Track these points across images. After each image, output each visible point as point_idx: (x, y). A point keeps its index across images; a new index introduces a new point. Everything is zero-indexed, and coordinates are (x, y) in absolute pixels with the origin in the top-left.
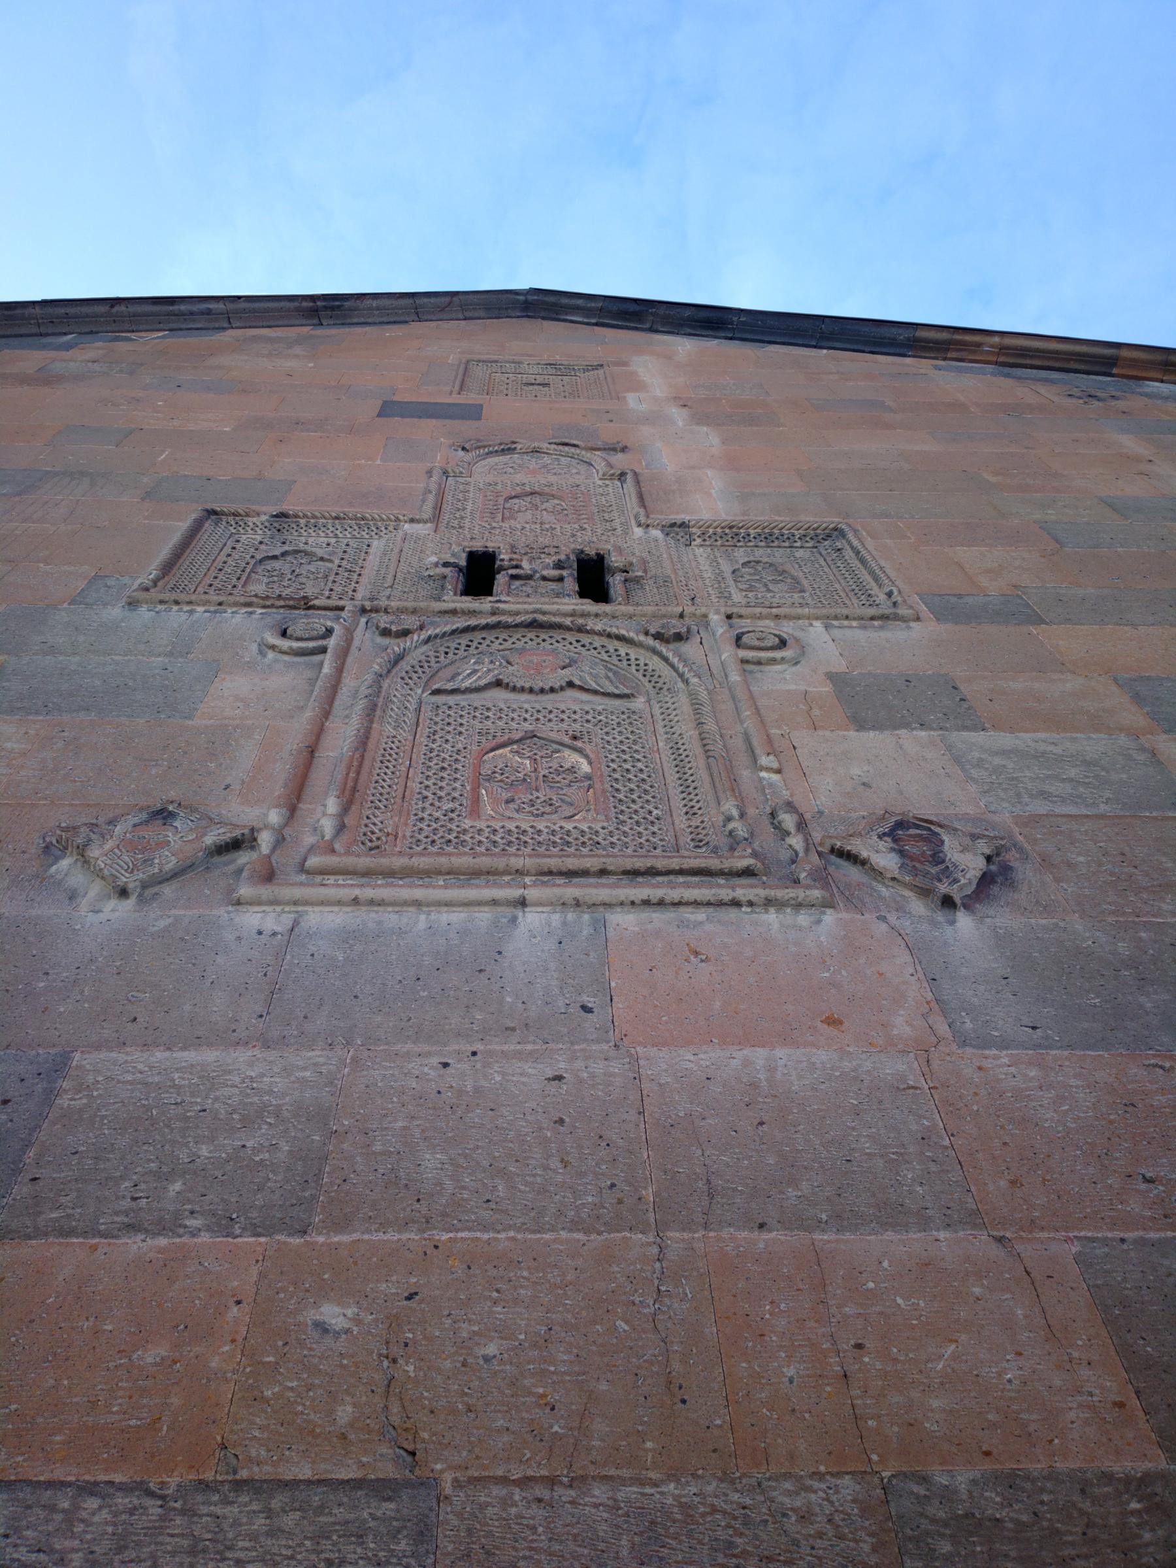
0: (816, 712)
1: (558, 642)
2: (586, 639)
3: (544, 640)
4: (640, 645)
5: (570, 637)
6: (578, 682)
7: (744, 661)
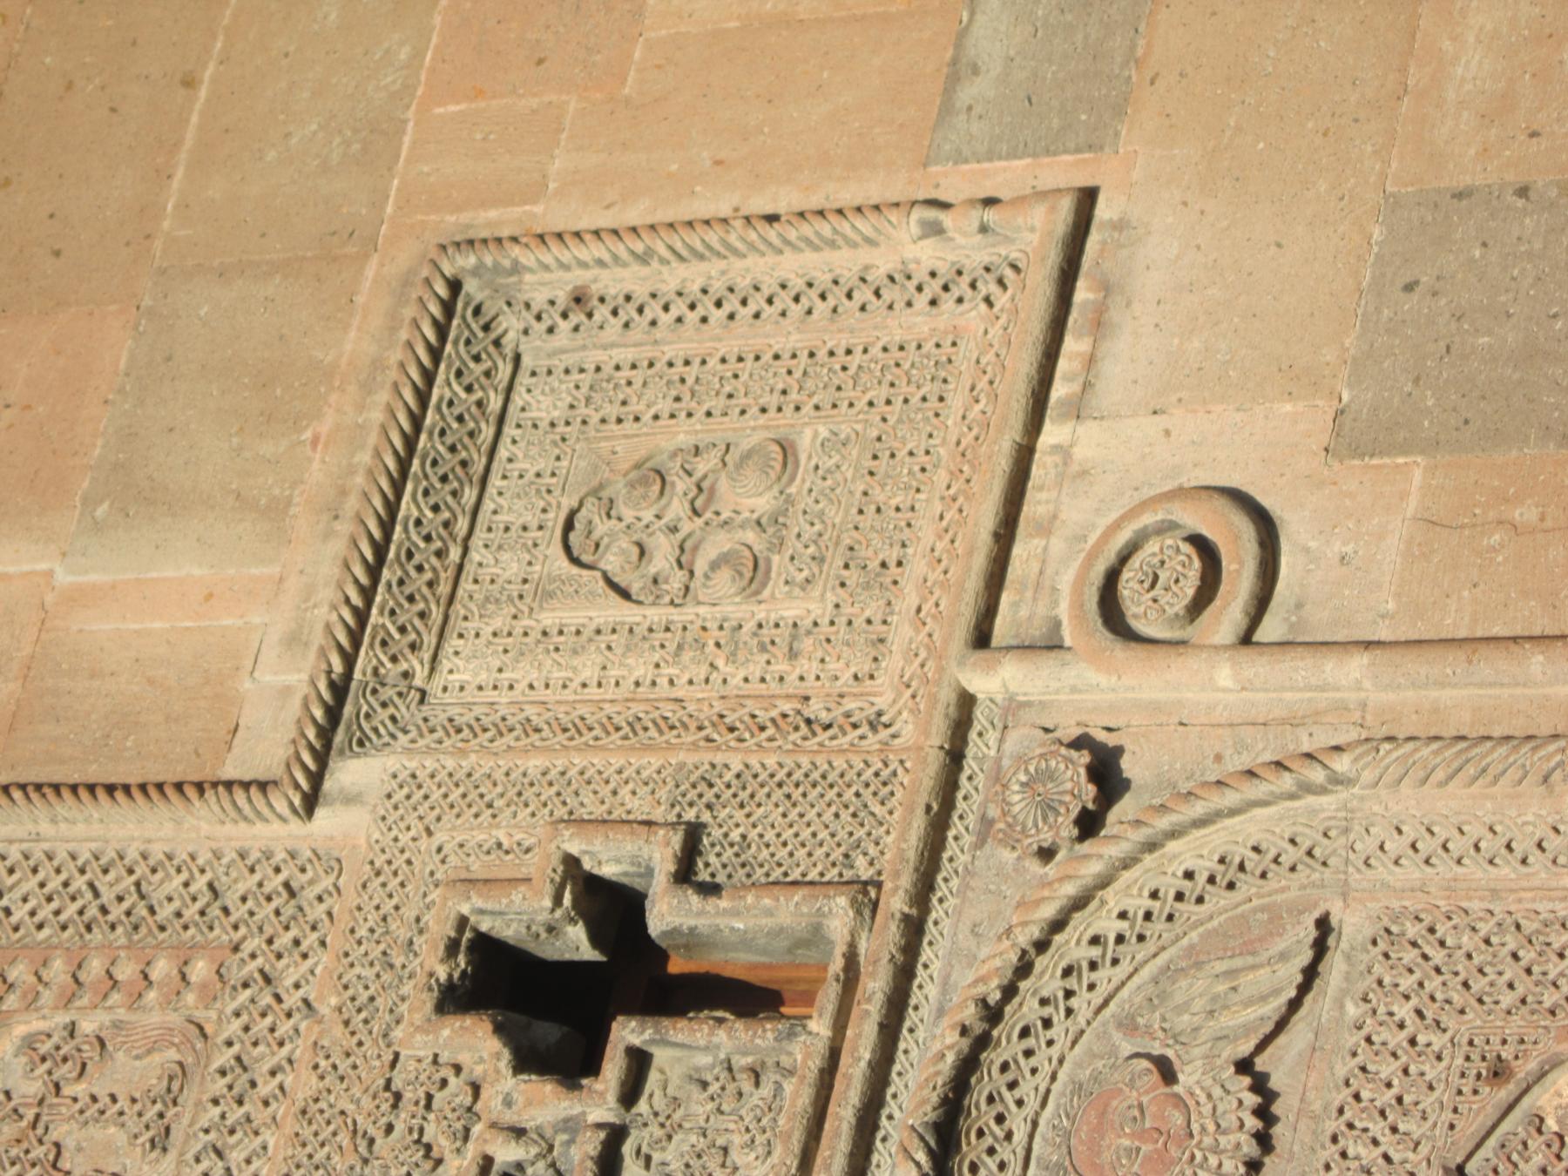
0: (1525, 513)
1: (1012, 1085)
2: (1026, 1009)
3: (1000, 1119)
4: (1104, 882)
5: (1007, 1046)
6: (1245, 1048)
7: (1246, 639)
